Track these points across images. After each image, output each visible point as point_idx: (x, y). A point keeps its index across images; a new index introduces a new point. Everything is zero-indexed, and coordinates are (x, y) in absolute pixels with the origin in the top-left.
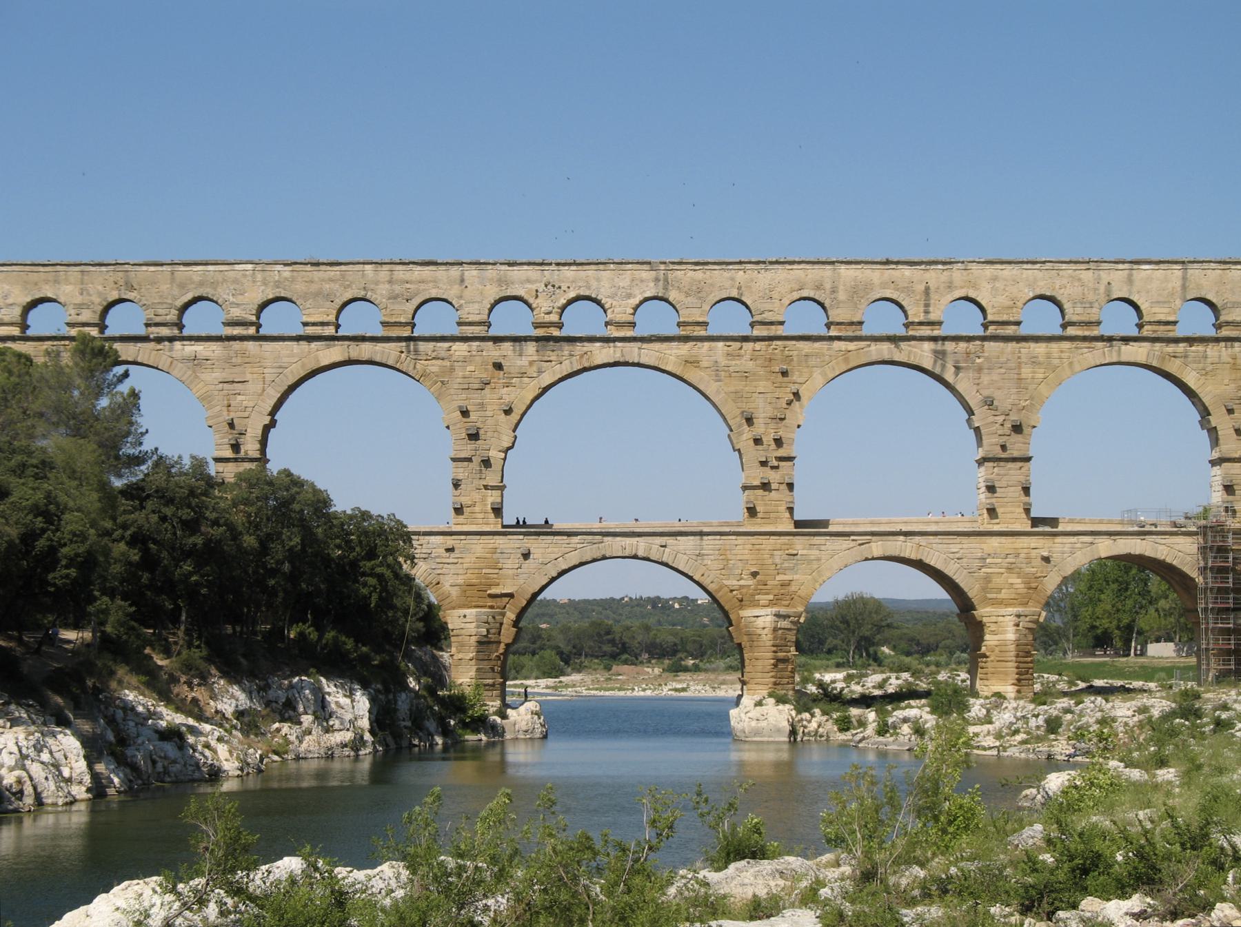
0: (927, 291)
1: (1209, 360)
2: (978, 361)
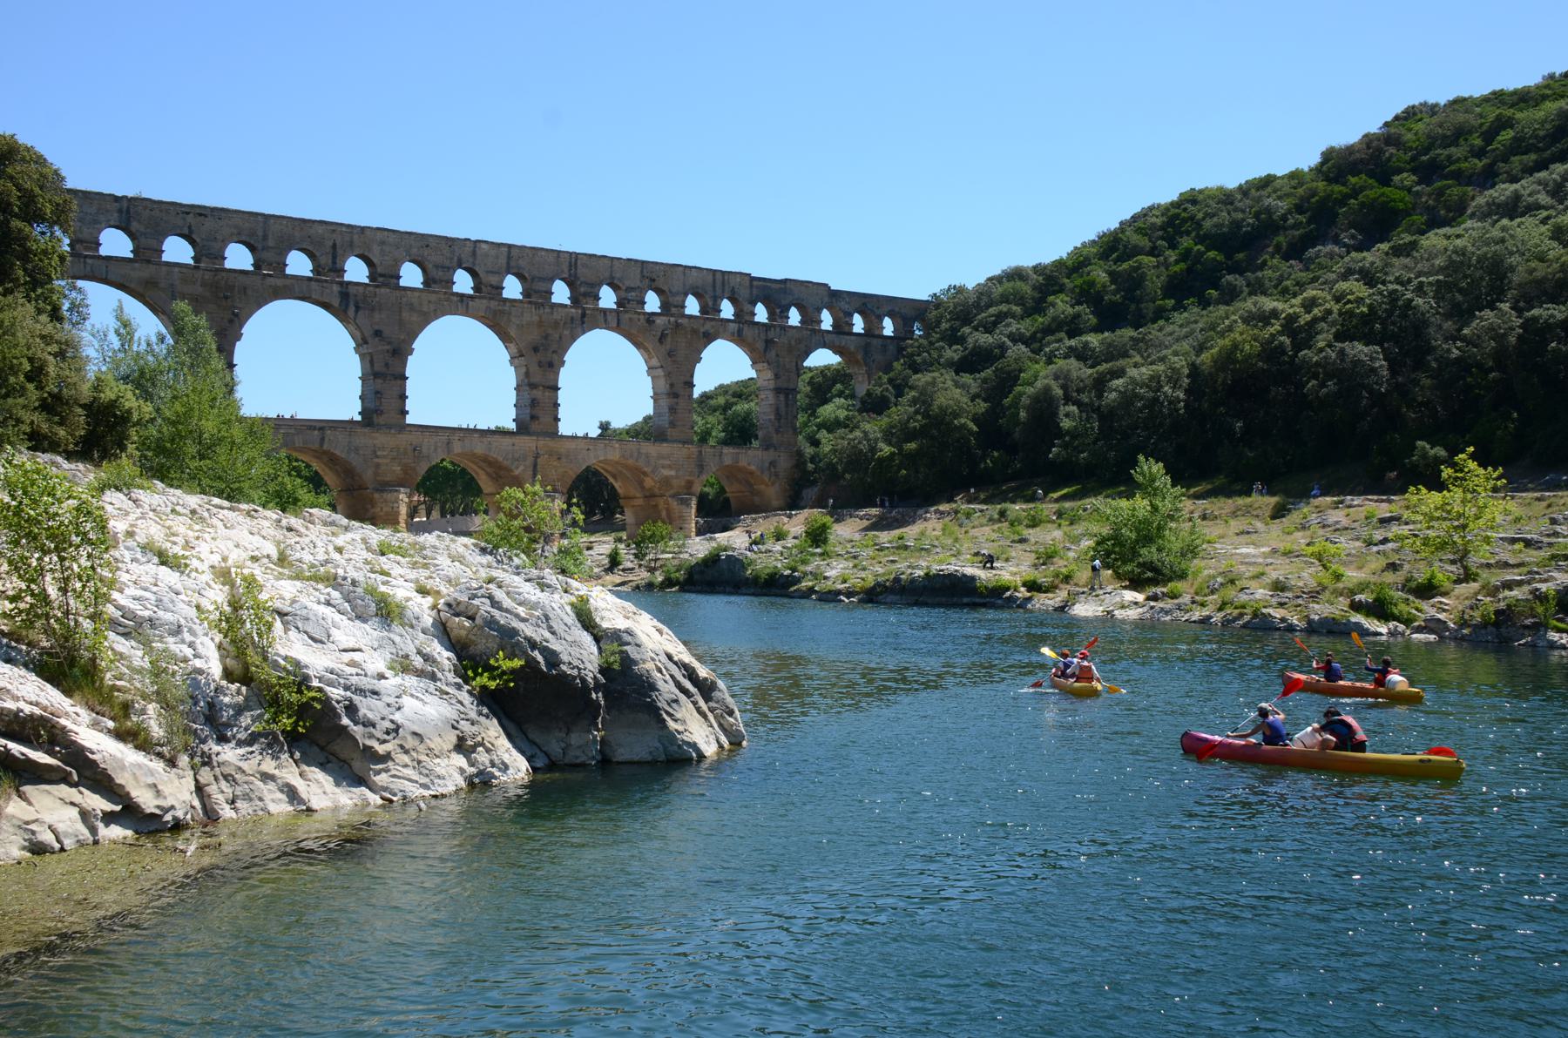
0: (334, 246)
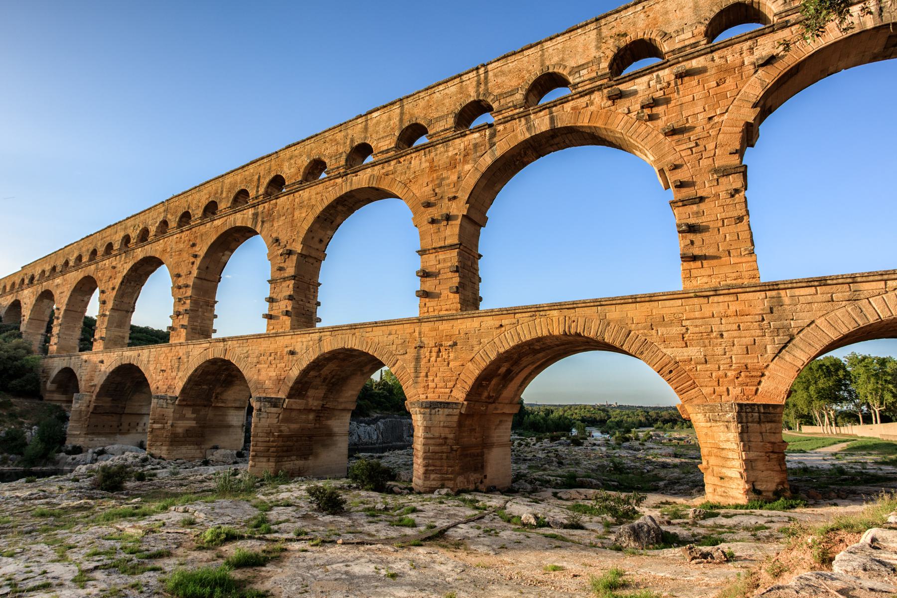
0: (259, 177)
1: (412, 170)
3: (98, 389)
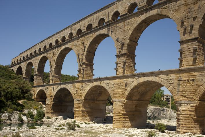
2: (116, 28)
3: (53, 97)
